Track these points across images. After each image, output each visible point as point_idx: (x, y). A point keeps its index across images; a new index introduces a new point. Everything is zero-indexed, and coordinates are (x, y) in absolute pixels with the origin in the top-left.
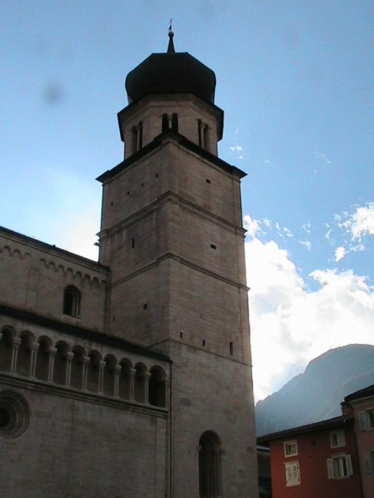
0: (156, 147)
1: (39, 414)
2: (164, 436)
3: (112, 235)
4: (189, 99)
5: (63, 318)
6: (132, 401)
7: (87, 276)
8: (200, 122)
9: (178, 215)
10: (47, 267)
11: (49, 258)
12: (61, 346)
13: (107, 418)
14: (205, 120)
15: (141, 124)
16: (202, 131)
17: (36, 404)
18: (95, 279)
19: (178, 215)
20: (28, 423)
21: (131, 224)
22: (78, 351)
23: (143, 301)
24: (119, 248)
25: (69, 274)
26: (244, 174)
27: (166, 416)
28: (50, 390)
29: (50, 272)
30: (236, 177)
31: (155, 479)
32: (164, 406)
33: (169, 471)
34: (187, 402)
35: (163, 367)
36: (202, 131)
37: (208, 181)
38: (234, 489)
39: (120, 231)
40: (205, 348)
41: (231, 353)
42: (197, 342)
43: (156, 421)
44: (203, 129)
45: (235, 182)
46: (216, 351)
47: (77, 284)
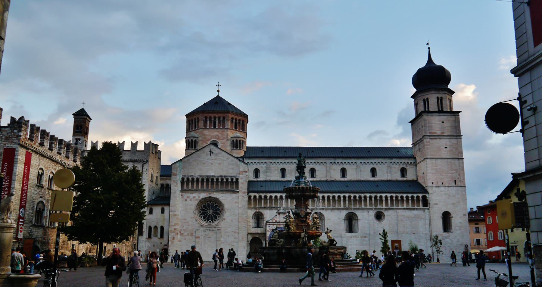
0: (420, 116)
1: (387, 215)
2: (428, 215)
3: (415, 145)
4: (431, 91)
5: (401, 179)
6: (416, 207)
7: (408, 163)
8: (438, 98)
9: (429, 142)
10: (393, 164)
11: (393, 161)
12: (391, 197)
13: (408, 213)
14: (440, 96)
15: (417, 103)
16: (440, 101)
17: (386, 213)
18: (411, 163)
19: (429, 142)
20: (385, 218)
21: (418, 143)
22: (397, 197)
23: (423, 171)
24: (417, 151)
25: (401, 164)
26: (460, 112)
27: (428, 209)
28: (389, 209)
29: (395, 165)
30: (456, 114)
31: (426, 227)
32: (427, 206)
33: (430, 225)
34: (436, 204)
35: (426, 195)
36: (440, 101)
37: (443, 122)
38: (457, 228)
39: (417, 144)
40: (443, 185)
41: (455, 184)
42: (440, 184)
43: (425, 211)
44: (440, 100)
45: (456, 116)
46: (448, 185)
47: (404, 166)
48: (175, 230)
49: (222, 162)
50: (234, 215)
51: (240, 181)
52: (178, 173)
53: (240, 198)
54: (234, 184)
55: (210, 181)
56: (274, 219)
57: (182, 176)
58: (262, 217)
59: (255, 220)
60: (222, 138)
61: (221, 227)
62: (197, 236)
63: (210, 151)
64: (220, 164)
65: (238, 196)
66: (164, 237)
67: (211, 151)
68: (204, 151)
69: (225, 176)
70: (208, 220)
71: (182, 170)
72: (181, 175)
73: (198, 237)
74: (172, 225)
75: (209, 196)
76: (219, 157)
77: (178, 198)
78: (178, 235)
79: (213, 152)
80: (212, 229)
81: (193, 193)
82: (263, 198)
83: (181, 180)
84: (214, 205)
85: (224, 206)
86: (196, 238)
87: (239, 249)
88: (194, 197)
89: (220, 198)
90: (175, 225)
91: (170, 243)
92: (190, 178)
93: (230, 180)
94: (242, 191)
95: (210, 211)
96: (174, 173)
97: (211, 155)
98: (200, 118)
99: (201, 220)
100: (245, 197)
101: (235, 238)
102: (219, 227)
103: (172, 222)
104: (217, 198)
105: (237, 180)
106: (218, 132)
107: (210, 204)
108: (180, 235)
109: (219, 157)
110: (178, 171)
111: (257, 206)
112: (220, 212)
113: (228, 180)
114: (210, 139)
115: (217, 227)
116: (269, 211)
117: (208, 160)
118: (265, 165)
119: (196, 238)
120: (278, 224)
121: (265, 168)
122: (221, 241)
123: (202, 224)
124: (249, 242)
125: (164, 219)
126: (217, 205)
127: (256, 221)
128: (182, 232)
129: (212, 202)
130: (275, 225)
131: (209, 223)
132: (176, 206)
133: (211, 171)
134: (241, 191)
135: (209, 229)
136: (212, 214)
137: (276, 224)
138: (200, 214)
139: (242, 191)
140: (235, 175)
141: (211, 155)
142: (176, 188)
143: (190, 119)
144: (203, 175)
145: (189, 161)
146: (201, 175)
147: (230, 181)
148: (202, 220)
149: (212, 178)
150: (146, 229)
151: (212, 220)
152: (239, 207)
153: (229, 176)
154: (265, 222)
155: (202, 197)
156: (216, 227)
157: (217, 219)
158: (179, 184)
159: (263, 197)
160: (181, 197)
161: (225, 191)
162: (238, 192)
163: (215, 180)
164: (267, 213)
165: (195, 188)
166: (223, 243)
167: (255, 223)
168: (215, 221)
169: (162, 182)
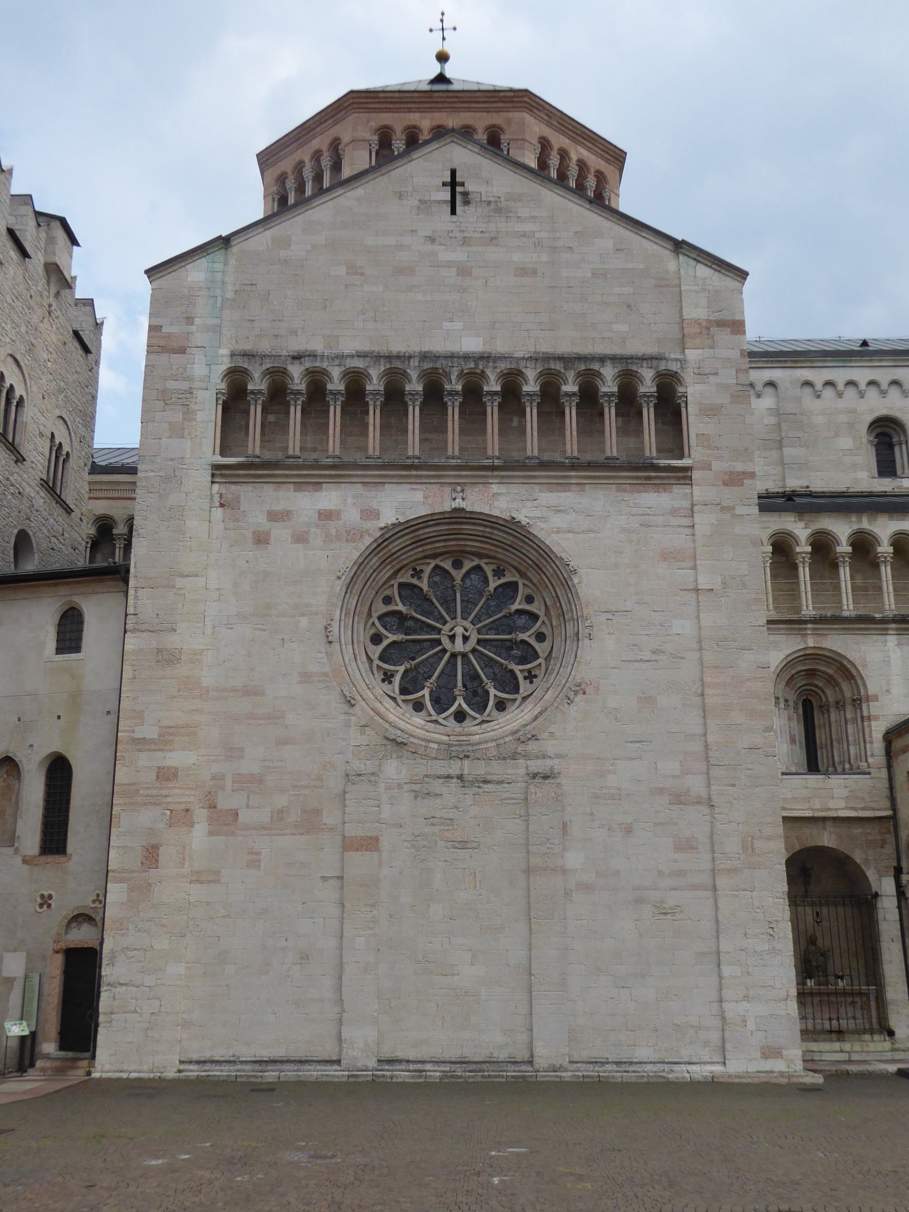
48: (168, 779)
49: (544, 258)
52: (199, 338)
53: (704, 521)
54: (649, 415)
55: (452, 393)
57: (233, 355)
58: (848, 694)
59: (790, 719)
61: (559, 756)
62: (353, 830)
63: (444, 184)
64: (523, 271)
65: (686, 504)
66: (73, 843)
67: (453, 184)
69: (568, 360)
70: (441, 703)
71: (227, 314)
72: (225, 351)
73: (370, 844)
74: (141, 744)
75: (448, 505)
76: (520, 227)
77: (194, 525)
78: (192, 824)
79: (470, 187)
80: (481, 769)
81: (317, 486)
82: (844, 548)
83: (223, 386)
84: (493, 585)
85: (576, 581)
86: (349, 845)
87: (723, 947)
88: (326, 516)
89: (542, 518)
91: (116, 893)
92: (296, 371)
93: (609, 384)
95: (459, 631)
96: (169, 336)
97: (453, 212)
98: (346, 138)
99: (389, 703)
100: (739, 510)
101: (684, 846)
102: (544, 757)
103: (139, 716)
104: (512, 526)
107: (458, 575)
108: (210, 819)
109: (520, 227)
110: (197, 321)
111: (808, 609)
112: (541, 637)
113: (596, 389)
115: (527, 757)
116: (899, 645)
117: (437, 248)
119: (349, 845)
121: (773, 420)
122: (565, 872)
123: (393, 733)
125: (75, 699)
126: (513, 586)
127: (798, 729)
128: (225, 802)
129: (468, 565)
131: (452, 722)
132: (179, 582)
133: (458, 325)
134: (708, 467)
135: (454, 768)
136: (474, 651)
138: (376, 651)
139: (716, 466)
140: (651, 349)
141: (453, 212)
143: (287, 165)
144: (397, 347)
145: (283, 254)
146: (376, 348)
147: (608, 395)
148: (394, 699)
149: (472, 373)
151: (479, 701)
152: (697, 590)
153: (602, 359)
154: (878, 730)
155: (389, 517)
156: (514, 756)
157: (516, 689)
160: (218, 513)
161: (575, 465)
162: (684, 475)
163: (498, 388)
164: (888, 663)
165: (334, 444)
166: (587, 888)
167: (793, 741)
168: (501, 706)
169: (101, 507)
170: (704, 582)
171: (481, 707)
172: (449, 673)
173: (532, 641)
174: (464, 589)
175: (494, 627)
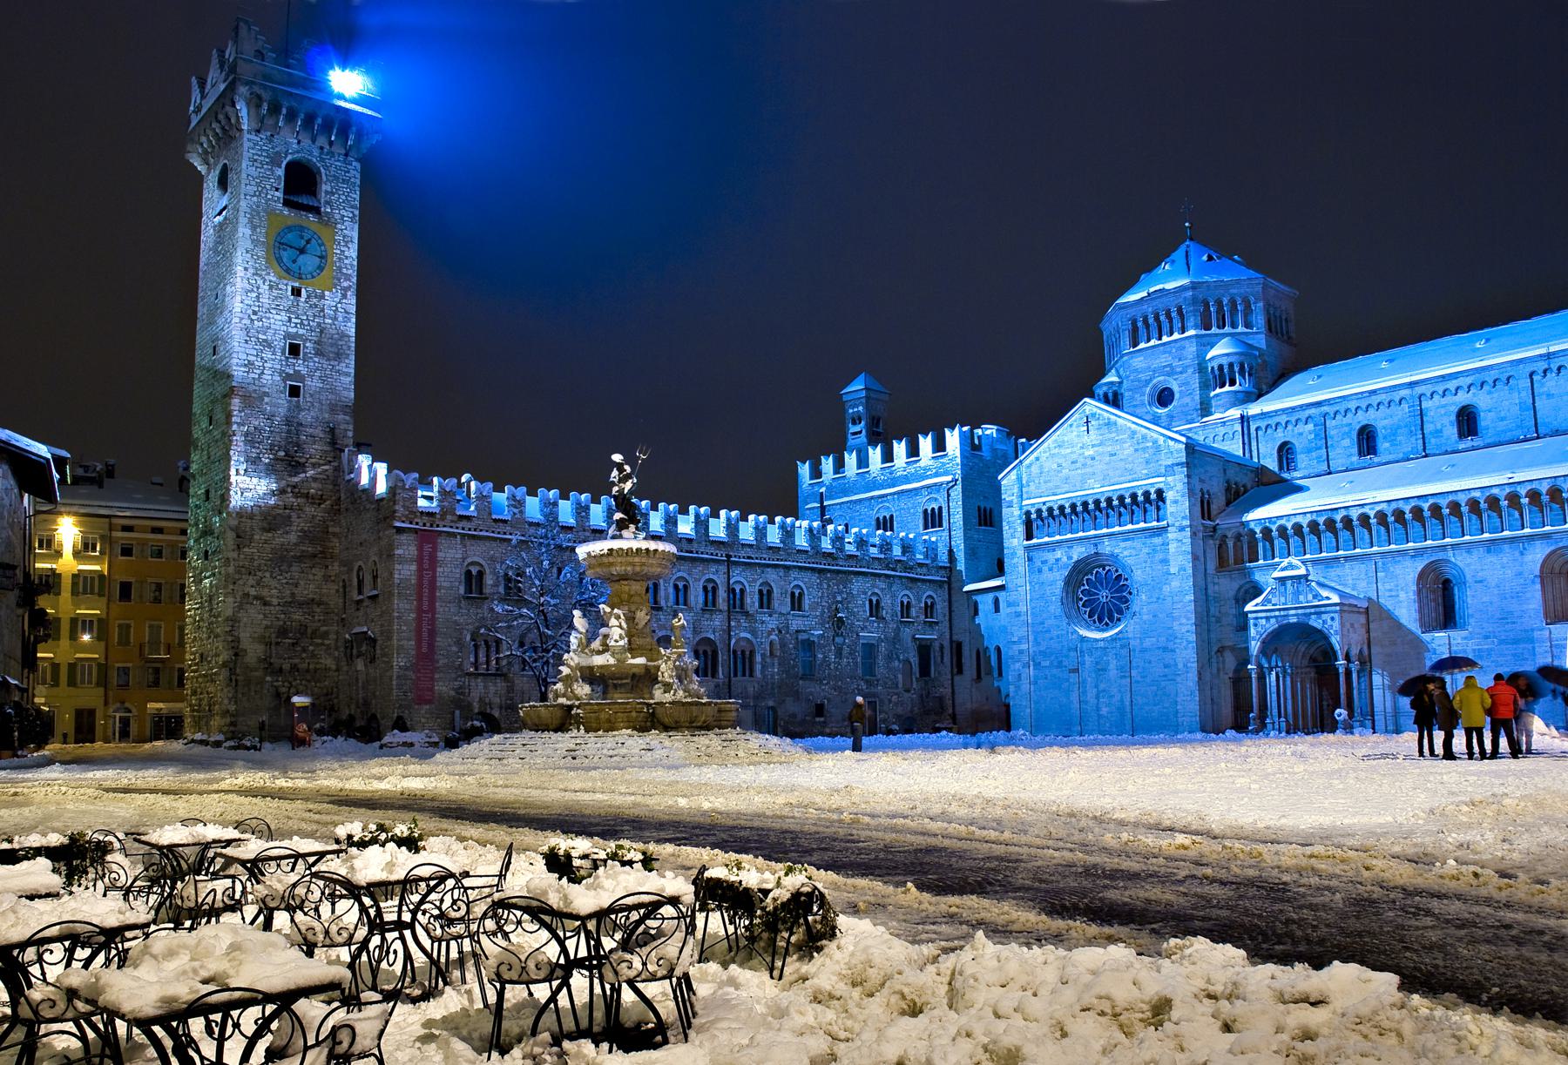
50: (1158, 598)
51: (1169, 495)
53: (1172, 547)
56: (1269, 601)
60: (1179, 370)
64: (1112, 455)
67: (1087, 422)
68: (1071, 426)
70: (1100, 620)
88: (1057, 560)
90: (1019, 642)
94: (1177, 524)
100: (1184, 541)
105: (1160, 493)
106: (1170, 352)
114: (1151, 380)
118: (1310, 426)
120: (1282, 613)
124: (1231, 675)
129: (1107, 568)
130: (1272, 617)
134: (1173, 525)
137: (1277, 613)
138: (1081, 603)
142: (1014, 539)
150: (971, 656)
155: (1075, 558)
158: (1021, 529)
159: (1258, 532)
166: (1138, 682)
168: (1119, 620)
170: (1172, 571)
171: (1112, 622)
172: (1103, 607)
173: (1128, 596)
174: (1106, 578)
175: (1116, 592)
